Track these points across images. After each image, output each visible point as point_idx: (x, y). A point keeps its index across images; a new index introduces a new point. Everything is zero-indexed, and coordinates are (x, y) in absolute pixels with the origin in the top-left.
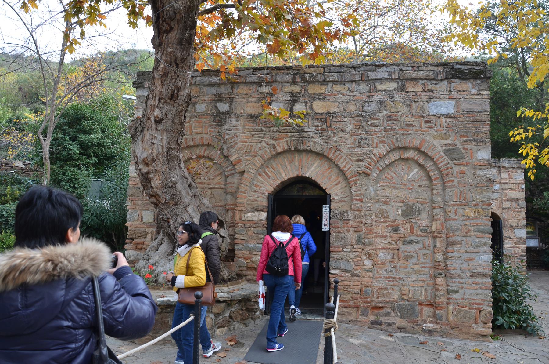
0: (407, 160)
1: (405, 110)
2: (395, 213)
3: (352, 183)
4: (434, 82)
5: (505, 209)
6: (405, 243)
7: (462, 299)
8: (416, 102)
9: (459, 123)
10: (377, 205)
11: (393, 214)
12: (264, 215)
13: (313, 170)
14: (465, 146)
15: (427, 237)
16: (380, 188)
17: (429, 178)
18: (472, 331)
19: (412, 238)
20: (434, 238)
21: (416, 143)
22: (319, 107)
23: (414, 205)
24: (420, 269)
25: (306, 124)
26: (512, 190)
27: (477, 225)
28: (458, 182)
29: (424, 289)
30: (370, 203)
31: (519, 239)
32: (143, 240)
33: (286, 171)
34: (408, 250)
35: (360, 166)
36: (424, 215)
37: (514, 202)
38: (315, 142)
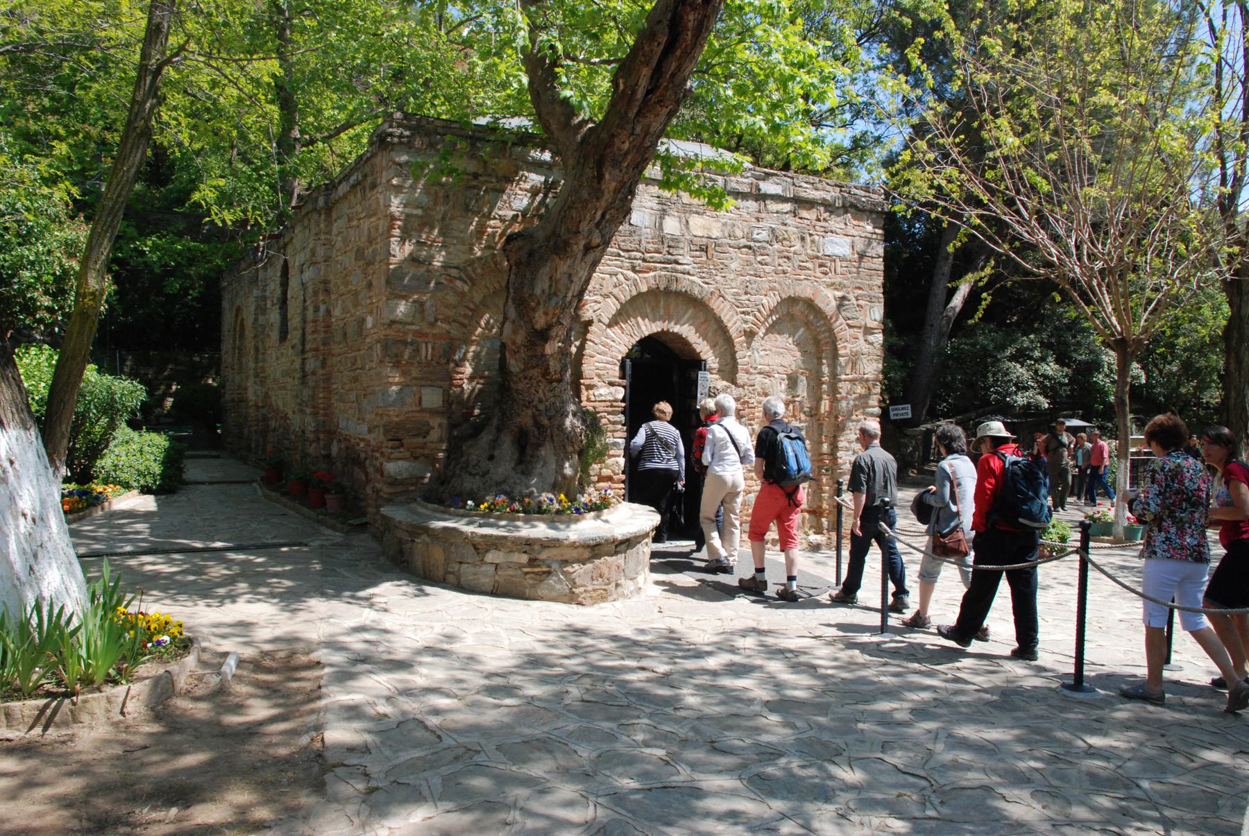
12: (620, 393)
14: (861, 302)
17: (817, 342)
32: (420, 440)
35: (746, 322)
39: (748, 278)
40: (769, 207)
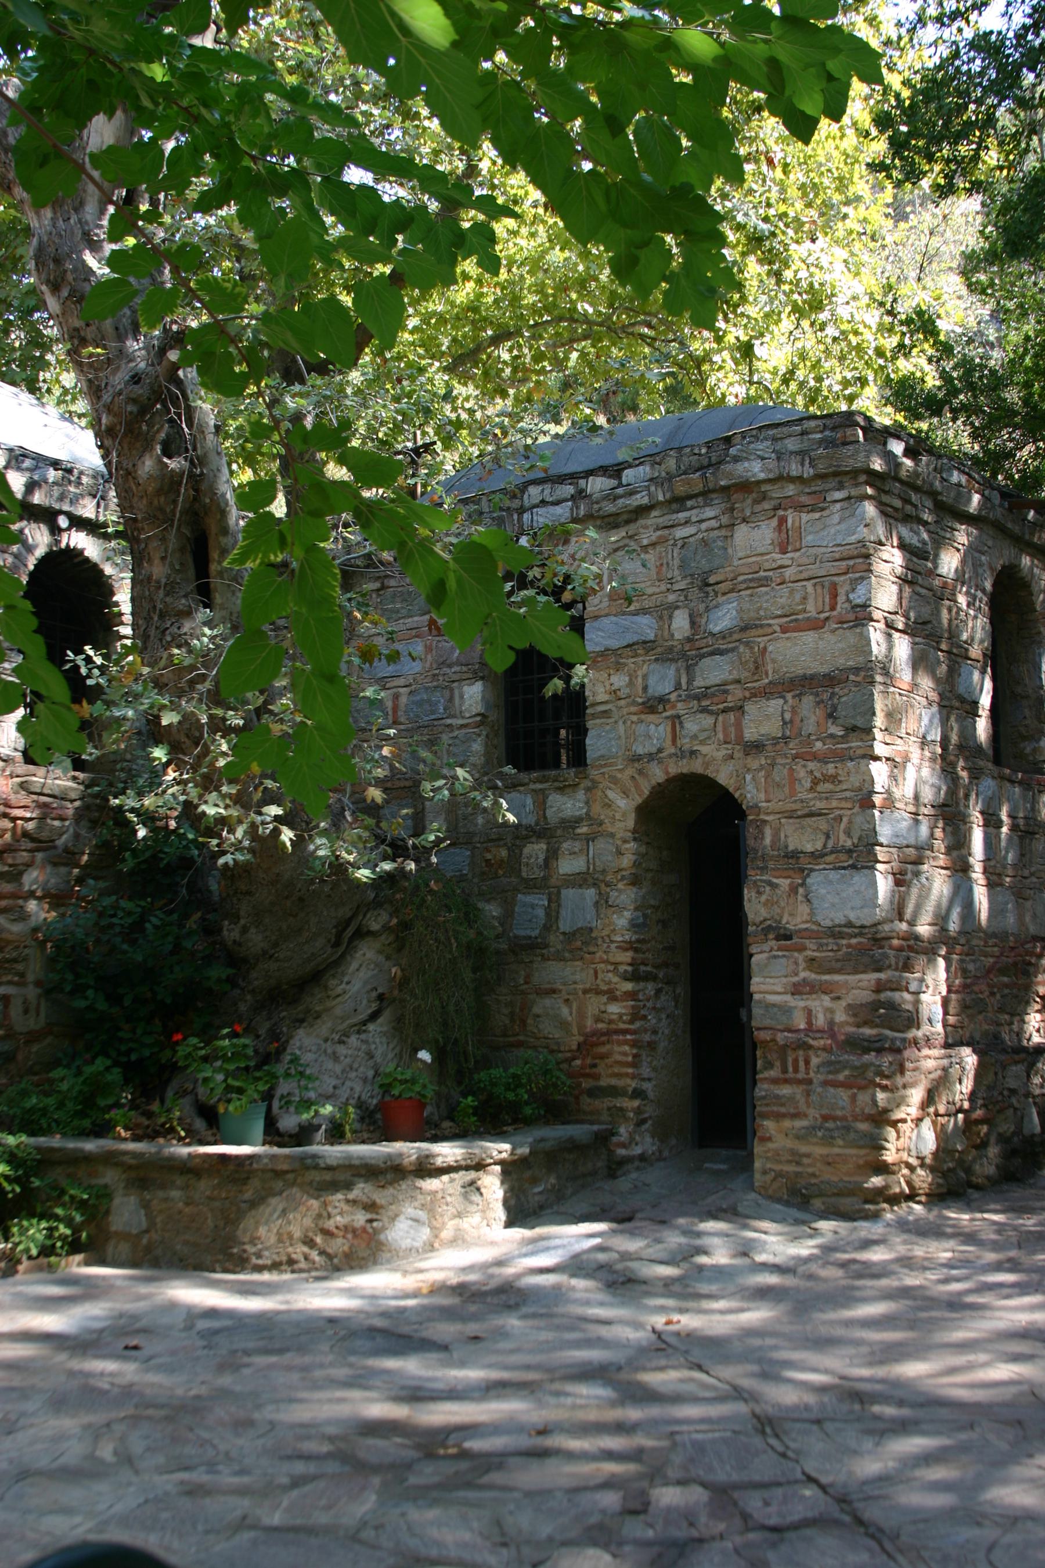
26: (796, 623)
31: (835, 932)
37: (808, 700)
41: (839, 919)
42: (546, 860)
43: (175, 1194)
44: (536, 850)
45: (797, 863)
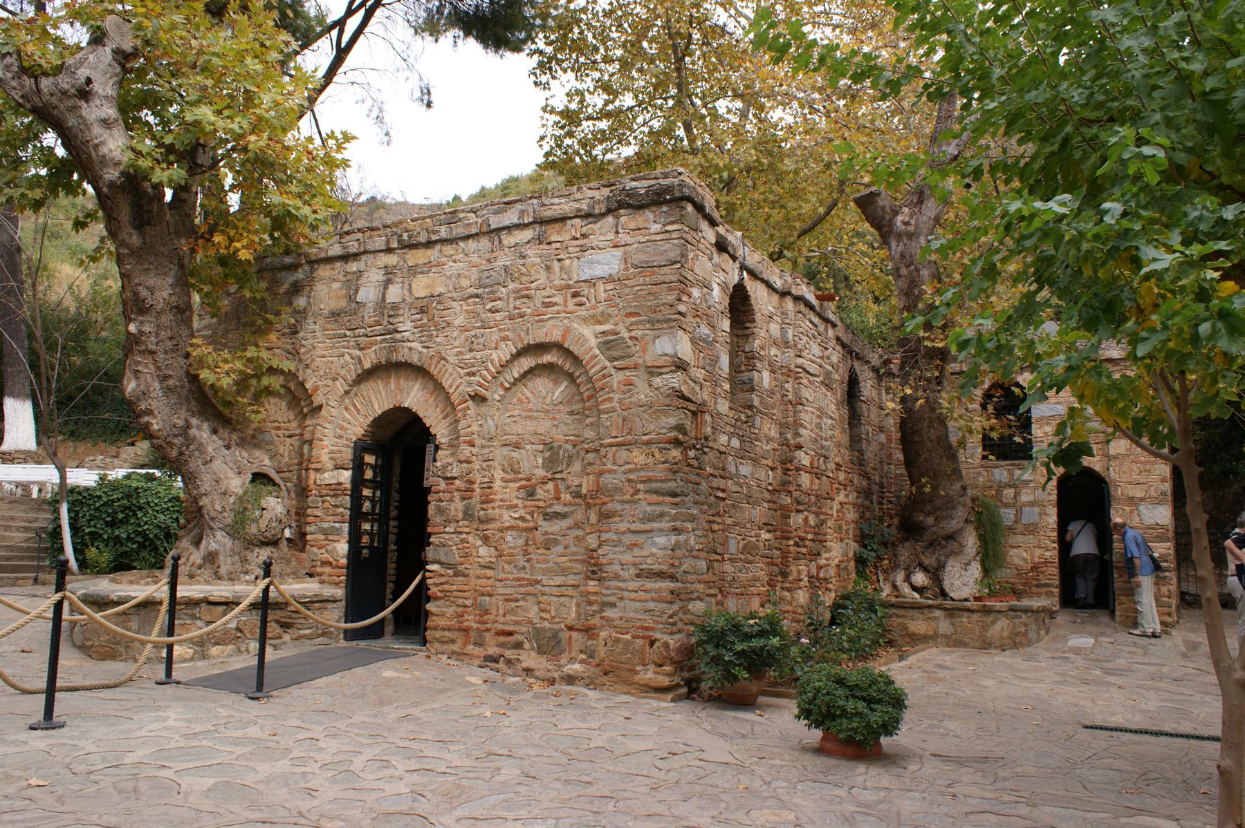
0: (550, 368)
1: (542, 279)
2: (532, 463)
3: (460, 415)
4: (591, 220)
5: (1116, 457)
6: (549, 517)
7: (621, 619)
8: (559, 260)
9: (627, 290)
10: (505, 450)
11: (527, 464)
12: (346, 476)
13: (414, 397)
14: (633, 334)
15: (580, 505)
16: (509, 420)
18: (637, 678)
19: (558, 508)
20: (588, 506)
21: (556, 336)
22: (421, 287)
23: (560, 447)
24: (569, 564)
25: (401, 319)
27: (649, 480)
28: (620, 401)
29: (574, 601)
30: (489, 447)
33: (380, 398)
34: (550, 530)
35: (470, 384)
36: (577, 467)
38: (410, 349)
39: (473, 333)
40: (505, 242)
41: (1153, 522)
42: (1015, 497)
43: (965, 620)
44: (1009, 493)
45: (1133, 501)
